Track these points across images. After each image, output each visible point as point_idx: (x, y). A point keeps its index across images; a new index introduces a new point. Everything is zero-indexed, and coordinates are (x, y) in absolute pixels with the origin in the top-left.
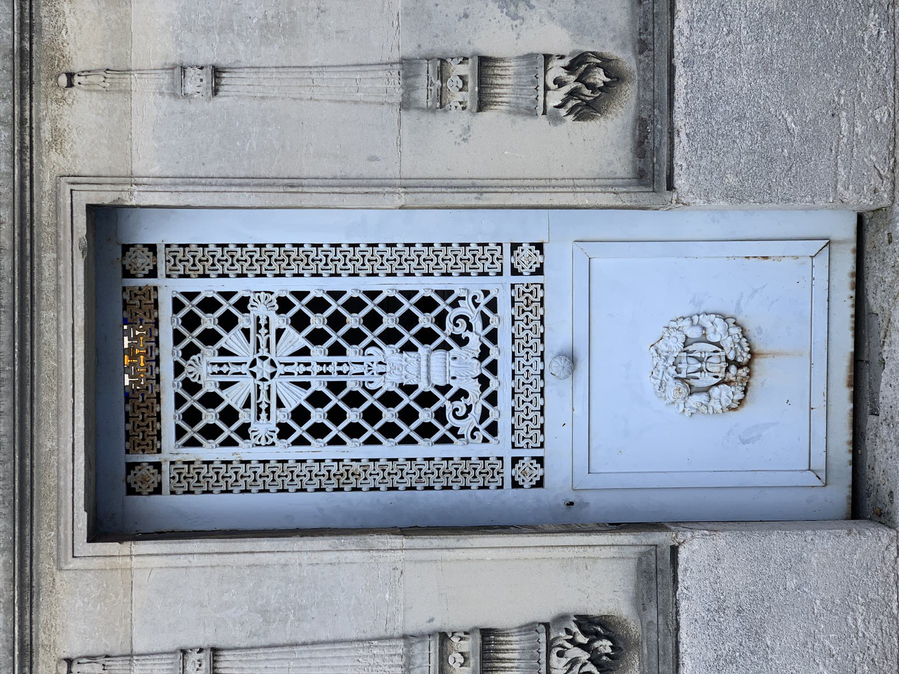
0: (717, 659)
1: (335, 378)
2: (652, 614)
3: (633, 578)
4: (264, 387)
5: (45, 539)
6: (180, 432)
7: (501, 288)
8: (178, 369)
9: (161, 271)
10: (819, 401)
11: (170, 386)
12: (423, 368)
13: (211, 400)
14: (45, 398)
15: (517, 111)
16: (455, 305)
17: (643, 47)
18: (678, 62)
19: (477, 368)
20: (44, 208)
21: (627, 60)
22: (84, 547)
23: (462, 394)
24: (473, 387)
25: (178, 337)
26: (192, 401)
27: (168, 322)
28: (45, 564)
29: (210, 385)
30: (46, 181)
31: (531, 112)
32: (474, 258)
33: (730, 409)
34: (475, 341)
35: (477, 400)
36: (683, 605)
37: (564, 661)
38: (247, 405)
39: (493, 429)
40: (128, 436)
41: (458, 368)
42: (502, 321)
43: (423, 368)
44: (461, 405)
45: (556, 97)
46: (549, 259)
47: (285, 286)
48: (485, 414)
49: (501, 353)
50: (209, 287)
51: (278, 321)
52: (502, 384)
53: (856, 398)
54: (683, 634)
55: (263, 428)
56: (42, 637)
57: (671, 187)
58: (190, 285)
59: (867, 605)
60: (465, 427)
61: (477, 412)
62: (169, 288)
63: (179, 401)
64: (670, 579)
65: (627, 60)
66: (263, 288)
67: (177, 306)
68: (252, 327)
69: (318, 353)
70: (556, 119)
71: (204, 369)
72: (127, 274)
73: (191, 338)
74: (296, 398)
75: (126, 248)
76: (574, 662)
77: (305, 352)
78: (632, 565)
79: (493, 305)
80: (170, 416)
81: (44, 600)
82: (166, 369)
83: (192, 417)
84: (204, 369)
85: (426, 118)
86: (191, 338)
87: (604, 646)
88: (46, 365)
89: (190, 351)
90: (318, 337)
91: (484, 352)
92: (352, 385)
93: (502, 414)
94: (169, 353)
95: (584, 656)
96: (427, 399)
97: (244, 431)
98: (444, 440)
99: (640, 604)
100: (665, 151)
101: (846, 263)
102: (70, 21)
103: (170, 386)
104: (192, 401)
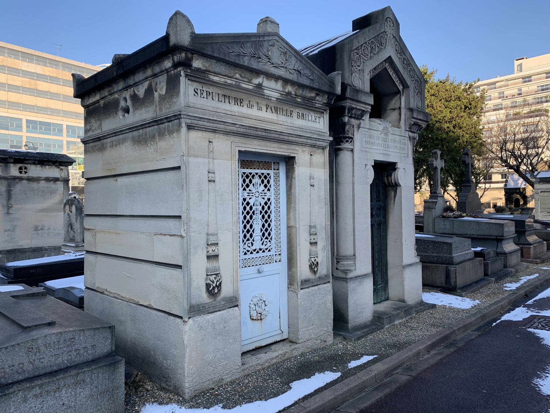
0: (214, 324)
1: (255, 212)
2: (223, 303)
3: (229, 296)
4: (253, 195)
5: (237, 139)
6: (244, 173)
7: (272, 252)
8: (257, 174)
9: (275, 171)
10: (253, 340)
11: (253, 171)
12: (257, 234)
13: (251, 181)
14: (263, 143)
15: (310, 251)
16: (270, 241)
17: (320, 278)
18: (318, 286)
19: (258, 248)
20: (293, 147)
21: (318, 275)
22: (238, 149)
23: (252, 244)
24: (253, 248)
25: (263, 174)
26: (250, 177)
27: (265, 172)
28: (232, 138)
29: (254, 181)
30: (297, 148)
31: (310, 255)
32: (278, 245)
33: (251, 317)
34: (263, 247)
35: (251, 249)
36: (225, 311)
37: (214, 279)
38: (250, 190)
39: (245, 254)
40: (244, 160)
41: (257, 245)
42: (267, 253)
43: (257, 234)
44: (250, 245)
45: (313, 260)
46: (278, 263)
47: (272, 200)
48: (248, 251)
49: (261, 254)
50: (272, 182)
51: (266, 200)
52: (255, 255)
53: (253, 350)
54: (219, 313)
55: (246, 194)
56: (217, 135)
57: (301, 289)
58: (272, 178)
59: (226, 365)
60: (246, 246)
61: (249, 249)
62: (271, 172)
63: (251, 173)
64: (231, 306)
65: (318, 275)
66: (271, 194)
67: (268, 174)
68: (265, 192)
69: (260, 208)
70: (309, 260)
71: (257, 180)
72: (274, 163)
73: (263, 177)
74: (252, 202)
75: (278, 163)
76: (213, 282)
77: (261, 205)
78: (232, 295)
79: (269, 251)
80: (247, 171)
81: (225, 137)
82: (251, 171)
83: (247, 177)
84: (257, 180)
85: (308, 231)
86: (263, 177)
87: (216, 291)
88: (268, 144)
89: (260, 177)
90: (263, 208)
91: (260, 249)
92: (254, 217)
93: (249, 256)
94: (260, 171)
95: (214, 285)
96: (251, 236)
97: (244, 189)
98: (243, 241)
99: (224, 299)
100: (306, 286)
101: (278, 338)
102: (319, 156)
103: (253, 171)
104: (250, 177)
